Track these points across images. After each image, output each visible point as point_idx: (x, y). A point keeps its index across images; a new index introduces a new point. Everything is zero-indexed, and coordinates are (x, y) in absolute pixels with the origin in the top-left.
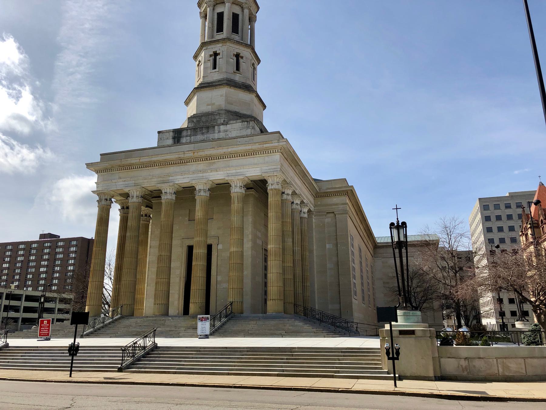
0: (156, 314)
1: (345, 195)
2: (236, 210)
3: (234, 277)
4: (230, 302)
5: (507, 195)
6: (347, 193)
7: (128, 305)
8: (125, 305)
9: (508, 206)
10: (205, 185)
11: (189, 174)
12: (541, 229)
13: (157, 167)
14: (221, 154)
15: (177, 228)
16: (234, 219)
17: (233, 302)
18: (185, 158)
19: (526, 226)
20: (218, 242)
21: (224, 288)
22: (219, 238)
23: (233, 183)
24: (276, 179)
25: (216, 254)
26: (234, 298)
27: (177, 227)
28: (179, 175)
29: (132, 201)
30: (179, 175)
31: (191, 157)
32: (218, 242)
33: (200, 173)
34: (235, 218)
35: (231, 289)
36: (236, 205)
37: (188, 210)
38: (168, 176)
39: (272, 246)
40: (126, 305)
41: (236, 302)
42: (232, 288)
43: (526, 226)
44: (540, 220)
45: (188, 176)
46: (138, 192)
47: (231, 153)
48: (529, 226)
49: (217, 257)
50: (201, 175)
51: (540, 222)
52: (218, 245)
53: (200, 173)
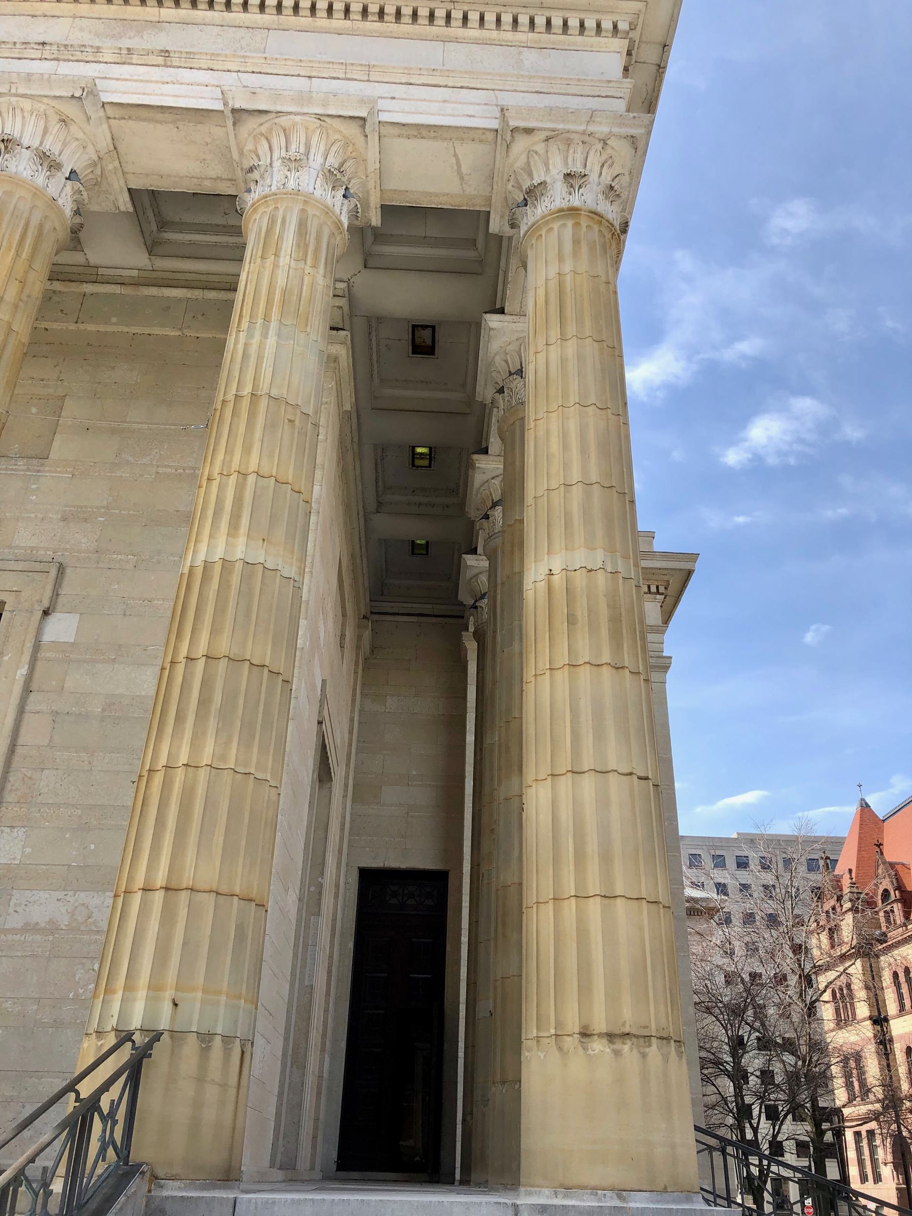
1: (658, 593)
2: (284, 292)
3: (203, 774)
4: (126, 1037)
5: (735, 836)
6: (666, 588)
9: (742, 864)
10: (55, 127)
12: (881, 914)
16: (261, 346)
17: (157, 1036)
19: (834, 908)
20: (56, 594)
21: (30, 928)
22: (68, 571)
24: (597, 168)
25: (23, 671)
26: (169, 994)
32: (56, 594)
33: (37, 55)
34: (271, 341)
35: (158, 897)
36: (284, 260)
39: (580, 558)
41: (191, 1045)
42: (160, 879)
43: (834, 908)
44: (880, 891)
48: (848, 905)
49: (27, 690)
50: (46, 67)
51: (880, 897)
52: (46, 613)
53: (37, 55)
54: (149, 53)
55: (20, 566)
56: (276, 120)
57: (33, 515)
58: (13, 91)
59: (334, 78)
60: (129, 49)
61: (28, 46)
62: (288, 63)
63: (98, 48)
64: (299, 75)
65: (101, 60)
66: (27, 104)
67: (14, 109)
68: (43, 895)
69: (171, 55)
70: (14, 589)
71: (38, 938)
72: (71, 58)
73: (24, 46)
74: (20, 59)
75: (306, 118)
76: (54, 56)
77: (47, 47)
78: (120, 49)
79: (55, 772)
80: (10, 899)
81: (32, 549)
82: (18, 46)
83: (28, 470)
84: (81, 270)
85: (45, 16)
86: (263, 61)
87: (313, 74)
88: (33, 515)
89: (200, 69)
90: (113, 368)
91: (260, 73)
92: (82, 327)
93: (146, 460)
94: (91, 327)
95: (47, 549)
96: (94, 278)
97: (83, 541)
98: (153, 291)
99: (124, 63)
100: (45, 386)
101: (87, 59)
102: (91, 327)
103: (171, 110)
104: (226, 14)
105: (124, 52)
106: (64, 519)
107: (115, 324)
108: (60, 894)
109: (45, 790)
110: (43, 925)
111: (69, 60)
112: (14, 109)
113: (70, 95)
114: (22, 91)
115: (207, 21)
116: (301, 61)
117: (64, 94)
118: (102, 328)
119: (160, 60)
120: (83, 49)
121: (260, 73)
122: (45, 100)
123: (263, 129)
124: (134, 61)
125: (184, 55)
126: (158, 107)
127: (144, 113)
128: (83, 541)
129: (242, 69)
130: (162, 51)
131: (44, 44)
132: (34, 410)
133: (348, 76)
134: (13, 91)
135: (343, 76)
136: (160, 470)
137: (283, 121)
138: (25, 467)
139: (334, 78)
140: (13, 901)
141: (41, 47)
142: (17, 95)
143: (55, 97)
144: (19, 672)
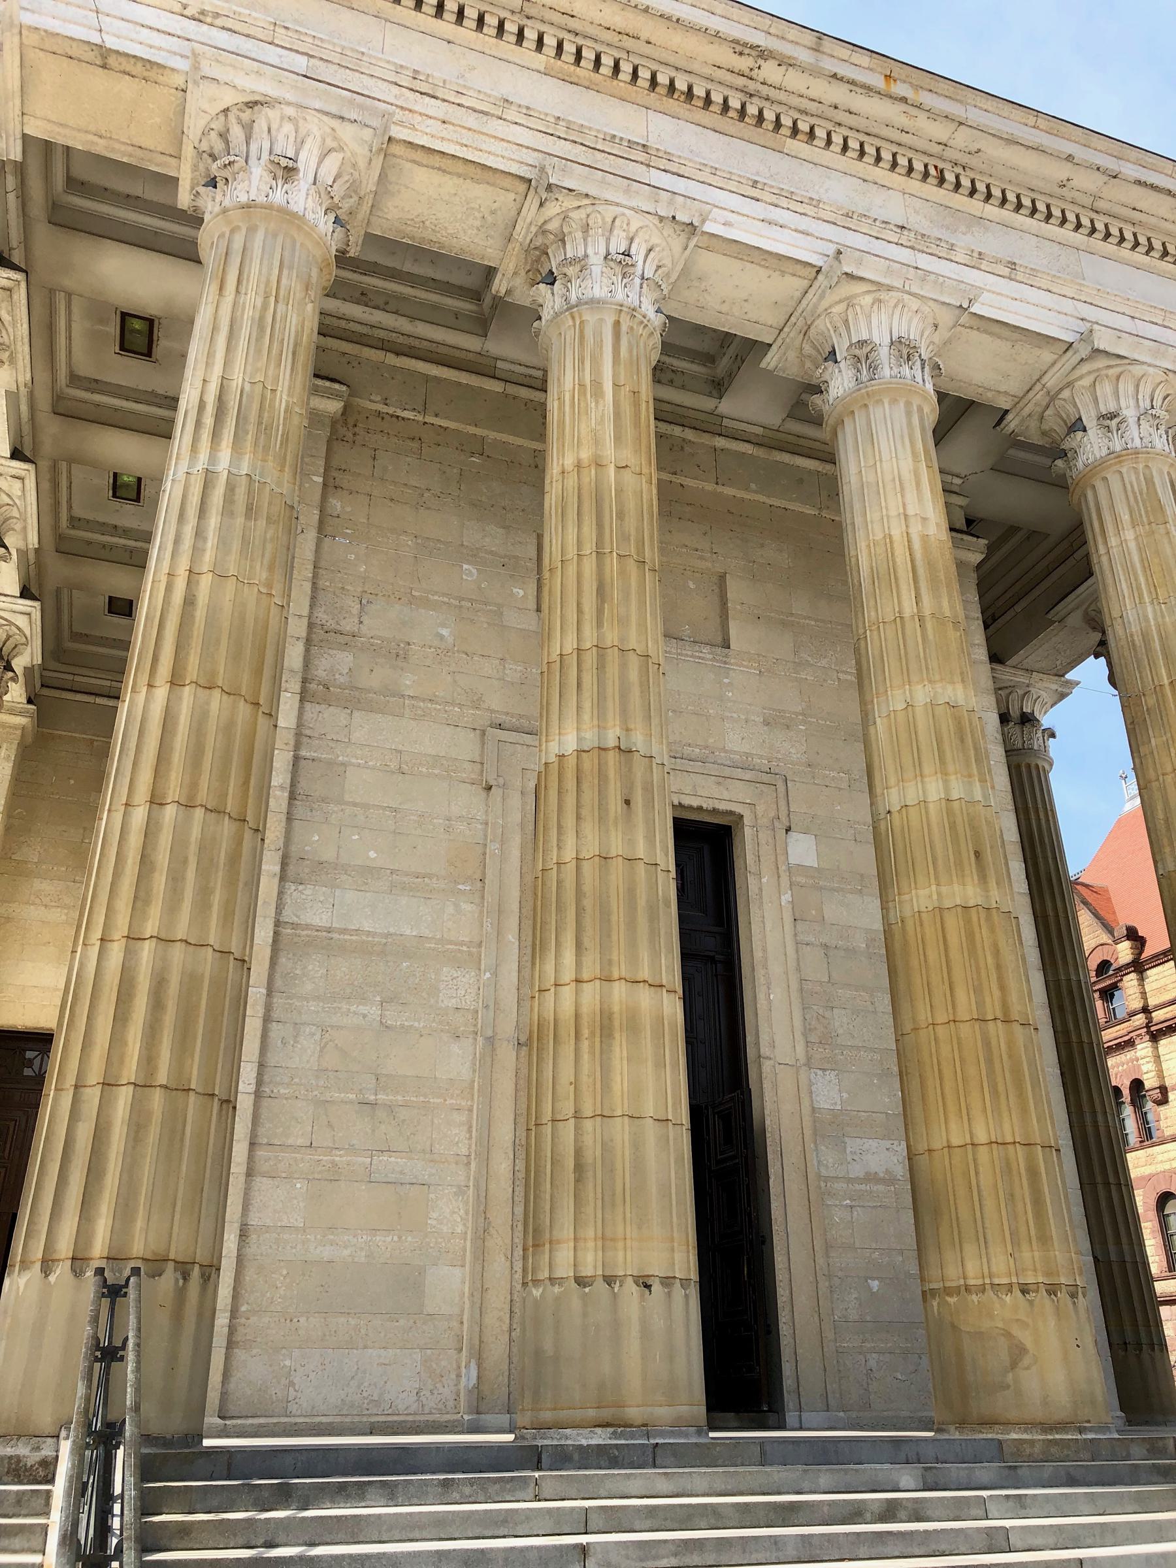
0: (634, 1413)
7: (196, 1271)
8: (156, 1264)
11: (810, 210)
13: (538, 61)
14: (1035, 184)
15: (442, 637)
18: (782, 96)
21: (871, 1178)
23: (1127, 387)
27: (445, 632)
28: (732, 186)
29: (278, 197)
30: (732, 186)
31: (831, 113)
37: (535, 535)
38: (642, 157)
40: (169, 1277)
45: (805, 223)
46: (331, 165)
47: (1100, 205)
54: (998, 261)
55: (748, 775)
56: (1130, 367)
57: (735, 715)
58: (907, 288)
59: (1153, 323)
60: (980, 254)
61: (888, 226)
62: (1117, 299)
63: (953, 245)
64: (1123, 314)
65: (953, 258)
66: (914, 304)
67: (903, 306)
68: (873, 1144)
69: (1017, 268)
70: (748, 801)
71: (881, 1188)
72: (925, 249)
73: (884, 226)
74: (877, 238)
75: (1156, 370)
76: (909, 244)
77: (906, 233)
78: (972, 251)
79: (843, 1012)
80: (845, 1148)
81: (747, 755)
82: (877, 223)
83: (714, 659)
84: (702, 416)
85: (876, 183)
86: (1095, 293)
87: (1137, 315)
88: (735, 715)
89: (1039, 288)
90: (762, 546)
91: (1091, 304)
92: (720, 489)
93: (824, 662)
94: (729, 491)
95: (761, 757)
96: (717, 429)
97: (793, 751)
98: (786, 458)
99: (973, 267)
100: (701, 558)
101: (940, 255)
102: (729, 491)
103: (1027, 333)
104: (1043, 224)
105: (976, 255)
106: (766, 723)
107: (756, 492)
108: (887, 1143)
109: (840, 1031)
110: (882, 1175)
111: (923, 252)
112: (903, 306)
113: (958, 304)
114: (915, 290)
115: (1024, 228)
116: (1128, 299)
117: (955, 303)
118: (740, 494)
119: (1006, 271)
120: (938, 243)
121: (1091, 304)
122: (931, 303)
123: (1111, 372)
124: (983, 267)
125: (1028, 271)
126: (1015, 327)
127: (996, 329)
128: (793, 751)
129: (1076, 297)
130: (1009, 262)
131: (903, 227)
132: (692, 585)
133: (1166, 324)
134: (907, 288)
135: (1160, 322)
136: (841, 676)
137: (1137, 370)
138: (710, 656)
139: (1153, 323)
140: (849, 1150)
141: (899, 231)
142: (910, 294)
143: (944, 303)
144: (782, 897)
